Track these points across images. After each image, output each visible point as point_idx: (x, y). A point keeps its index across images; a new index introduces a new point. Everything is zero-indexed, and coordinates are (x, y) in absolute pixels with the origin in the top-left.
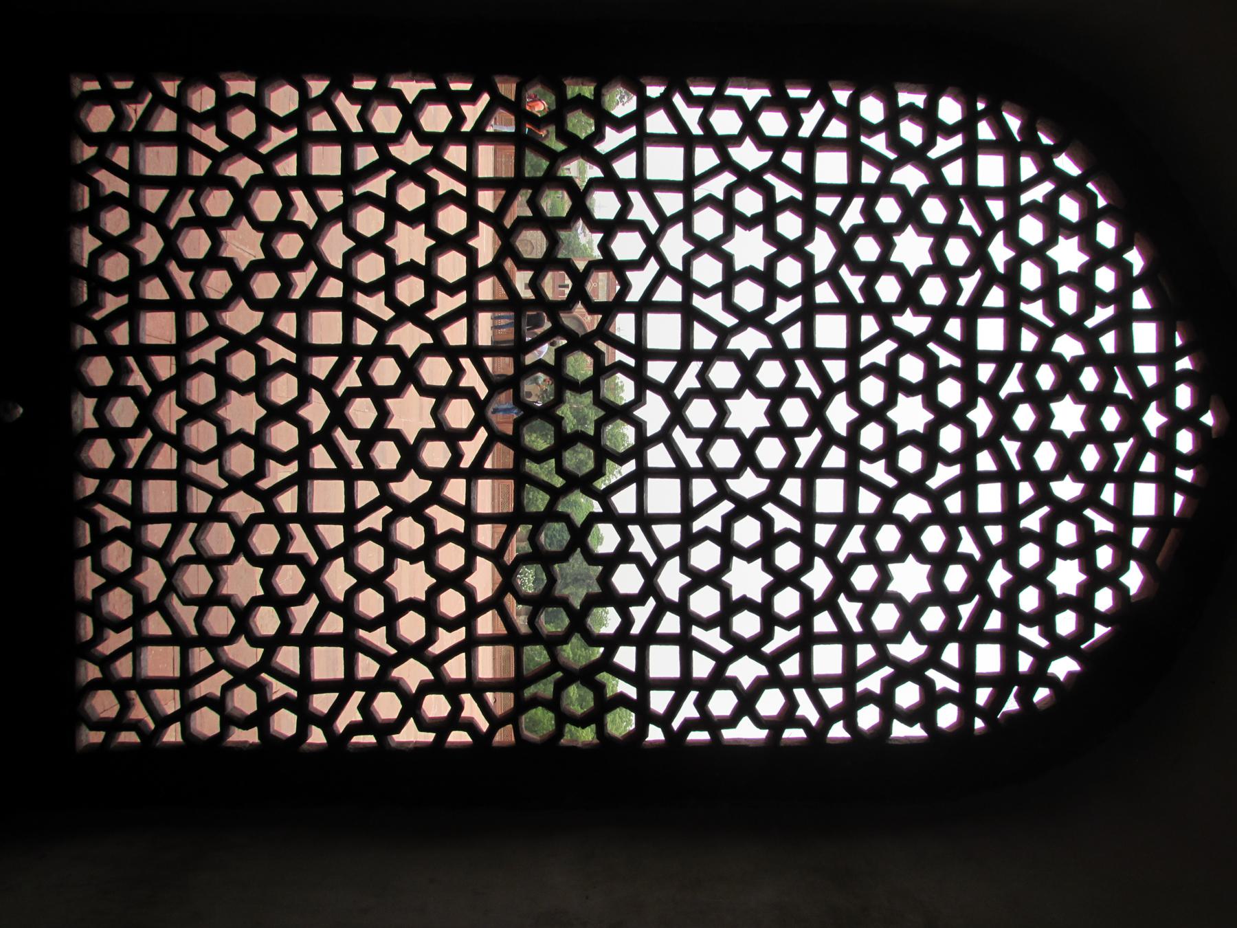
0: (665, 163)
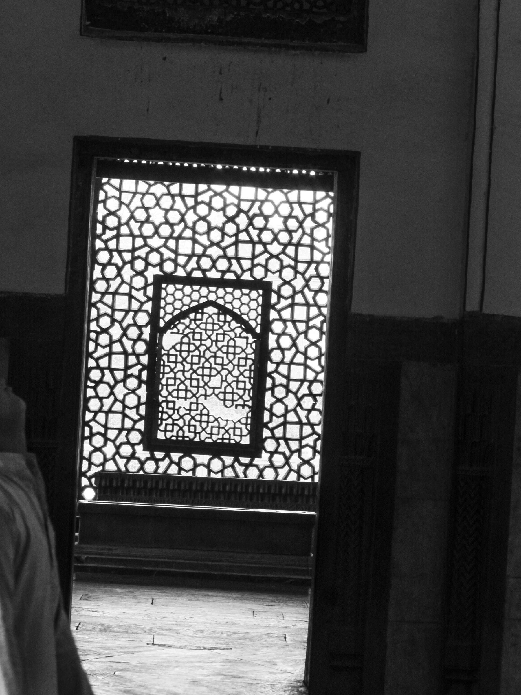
0: (126, 243)
